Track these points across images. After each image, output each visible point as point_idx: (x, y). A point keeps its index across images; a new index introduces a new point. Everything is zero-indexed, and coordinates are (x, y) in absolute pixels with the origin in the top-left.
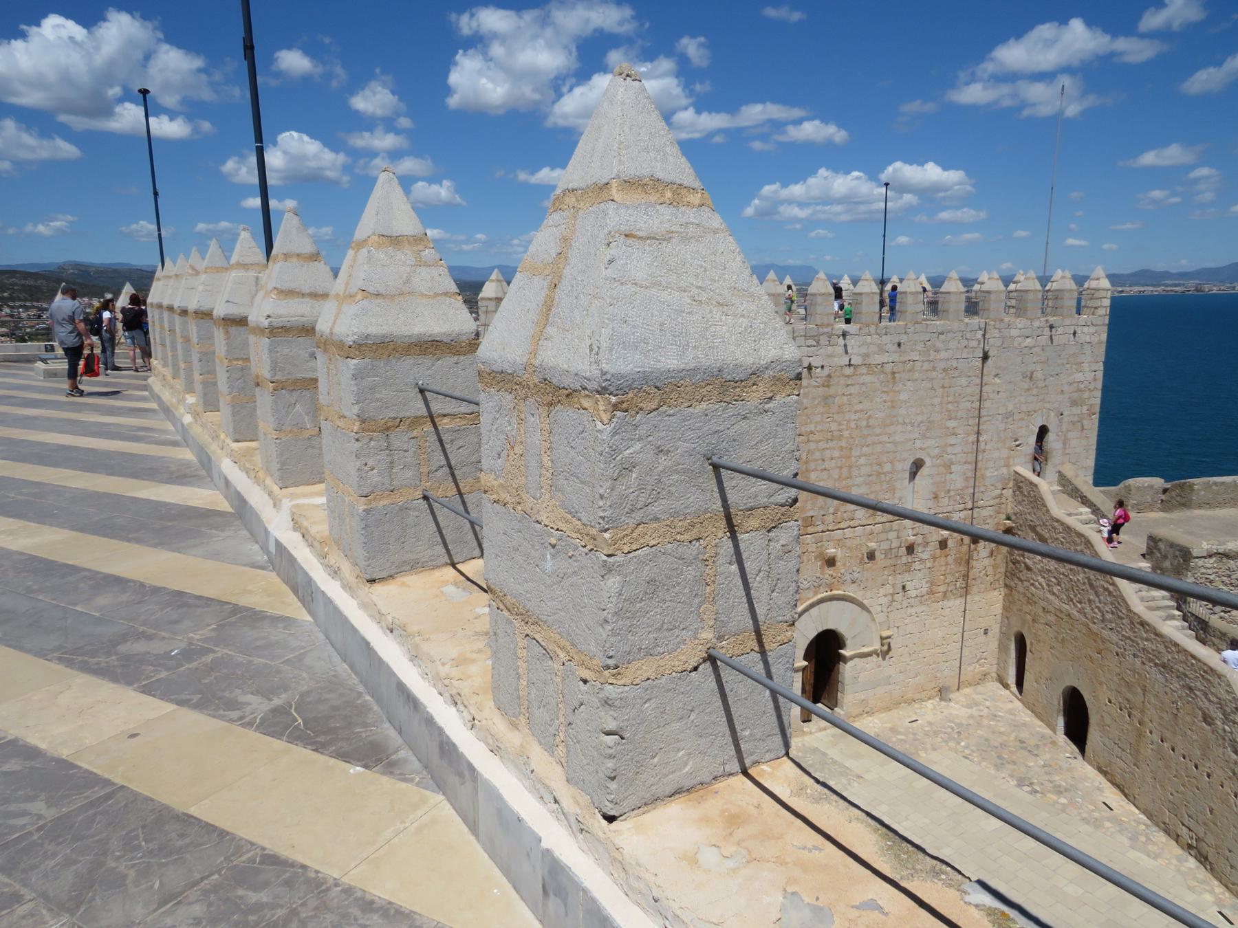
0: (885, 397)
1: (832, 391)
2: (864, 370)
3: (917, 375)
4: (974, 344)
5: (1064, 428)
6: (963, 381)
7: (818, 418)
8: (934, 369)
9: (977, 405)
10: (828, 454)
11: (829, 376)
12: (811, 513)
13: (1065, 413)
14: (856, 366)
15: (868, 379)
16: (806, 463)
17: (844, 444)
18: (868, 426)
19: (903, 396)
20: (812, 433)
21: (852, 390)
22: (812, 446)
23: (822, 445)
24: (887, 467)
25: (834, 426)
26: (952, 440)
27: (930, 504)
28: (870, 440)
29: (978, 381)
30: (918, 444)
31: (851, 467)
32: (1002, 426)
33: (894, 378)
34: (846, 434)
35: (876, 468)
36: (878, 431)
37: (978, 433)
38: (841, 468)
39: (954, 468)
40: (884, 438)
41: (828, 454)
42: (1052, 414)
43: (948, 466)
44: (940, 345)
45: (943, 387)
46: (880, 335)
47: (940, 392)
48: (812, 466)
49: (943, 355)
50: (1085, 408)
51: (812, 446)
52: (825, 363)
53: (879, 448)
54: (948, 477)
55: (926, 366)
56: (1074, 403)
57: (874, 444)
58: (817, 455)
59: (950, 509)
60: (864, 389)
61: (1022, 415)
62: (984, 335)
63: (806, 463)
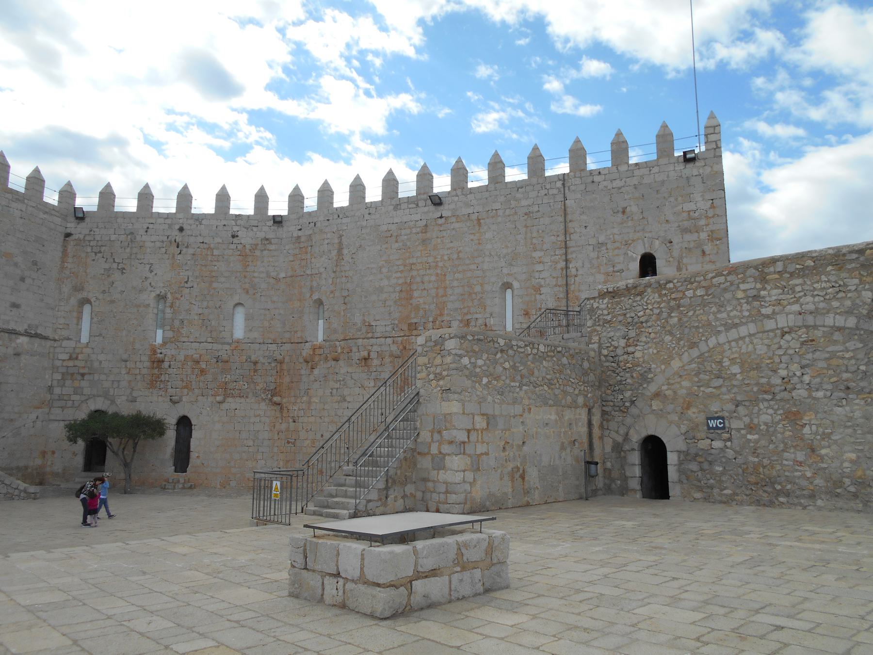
0: (472, 237)
1: (428, 235)
2: (454, 219)
3: (500, 219)
4: (555, 191)
5: (676, 253)
6: (547, 220)
7: (419, 254)
8: (516, 213)
9: (562, 238)
10: (426, 278)
11: (426, 226)
12: (415, 321)
13: (675, 241)
14: (447, 218)
15: (457, 225)
16: (411, 284)
17: (439, 271)
18: (459, 258)
19: (489, 235)
20: (414, 264)
21: (444, 234)
22: (414, 273)
23: (422, 272)
24: (478, 289)
25: (431, 260)
26: (540, 267)
27: (521, 319)
28: (460, 268)
29: (561, 219)
30: (505, 271)
31: (445, 288)
32: (593, 255)
33: (480, 224)
34: (441, 264)
35: (467, 289)
36: (467, 262)
37: (566, 260)
38: (437, 288)
39: (543, 290)
40: (473, 267)
41: (426, 278)
42: (657, 242)
43: (537, 289)
44: (519, 196)
45: (526, 227)
46: (466, 195)
47: (523, 230)
48: (414, 287)
49: (524, 203)
50: (703, 236)
51: (414, 273)
52: (423, 218)
53: (469, 274)
54: (538, 296)
55: (508, 212)
56: (685, 231)
57: (464, 271)
58: (418, 279)
59: (542, 324)
60: (454, 232)
61: (617, 245)
62: (563, 184)
63: (411, 284)
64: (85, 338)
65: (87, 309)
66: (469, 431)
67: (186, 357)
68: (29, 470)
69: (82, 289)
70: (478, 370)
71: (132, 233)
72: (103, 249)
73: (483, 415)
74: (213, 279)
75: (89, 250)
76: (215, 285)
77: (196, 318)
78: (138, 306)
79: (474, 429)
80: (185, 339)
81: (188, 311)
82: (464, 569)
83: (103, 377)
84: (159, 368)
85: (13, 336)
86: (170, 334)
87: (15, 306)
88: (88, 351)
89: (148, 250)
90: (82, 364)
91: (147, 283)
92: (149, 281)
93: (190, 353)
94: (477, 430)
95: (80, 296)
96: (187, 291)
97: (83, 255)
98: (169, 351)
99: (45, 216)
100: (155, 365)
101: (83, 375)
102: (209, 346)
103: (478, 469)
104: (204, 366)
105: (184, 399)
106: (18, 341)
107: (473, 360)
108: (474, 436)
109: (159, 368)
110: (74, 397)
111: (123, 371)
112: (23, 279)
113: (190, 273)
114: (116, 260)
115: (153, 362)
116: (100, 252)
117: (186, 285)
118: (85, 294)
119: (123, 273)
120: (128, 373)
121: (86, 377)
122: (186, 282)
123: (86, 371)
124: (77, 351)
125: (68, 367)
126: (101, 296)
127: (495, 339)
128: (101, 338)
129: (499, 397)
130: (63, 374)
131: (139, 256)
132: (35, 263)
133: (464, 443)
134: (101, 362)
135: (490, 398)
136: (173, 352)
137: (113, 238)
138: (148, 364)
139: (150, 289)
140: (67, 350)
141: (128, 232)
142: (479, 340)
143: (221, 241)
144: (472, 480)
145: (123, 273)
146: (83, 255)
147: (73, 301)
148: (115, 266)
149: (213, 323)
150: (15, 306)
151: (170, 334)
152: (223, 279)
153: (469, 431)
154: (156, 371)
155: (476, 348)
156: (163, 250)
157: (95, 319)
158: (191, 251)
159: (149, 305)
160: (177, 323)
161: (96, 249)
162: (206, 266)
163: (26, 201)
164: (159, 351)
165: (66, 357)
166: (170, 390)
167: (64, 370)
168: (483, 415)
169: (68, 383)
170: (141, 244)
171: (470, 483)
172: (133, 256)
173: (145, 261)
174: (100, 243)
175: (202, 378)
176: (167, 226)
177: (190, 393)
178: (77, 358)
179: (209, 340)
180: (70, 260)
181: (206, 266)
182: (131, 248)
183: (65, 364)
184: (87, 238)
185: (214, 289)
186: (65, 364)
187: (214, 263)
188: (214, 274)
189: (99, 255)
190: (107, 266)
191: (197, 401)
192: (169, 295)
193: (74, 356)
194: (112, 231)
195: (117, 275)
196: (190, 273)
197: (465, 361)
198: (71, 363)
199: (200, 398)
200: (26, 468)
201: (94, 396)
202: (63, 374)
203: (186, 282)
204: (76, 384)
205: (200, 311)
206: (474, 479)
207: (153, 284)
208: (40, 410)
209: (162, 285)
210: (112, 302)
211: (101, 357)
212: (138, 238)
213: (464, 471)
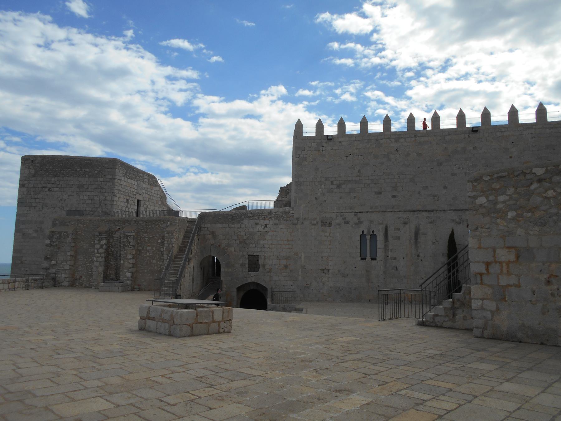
66: (488, 264)
70: (500, 206)
73: (509, 248)
79: (496, 262)
82: (162, 322)
94: (500, 263)
103: (503, 299)
107: (491, 198)
108: (494, 269)
127: (528, 171)
129: (537, 229)
133: (481, 274)
135: (520, 231)
142: (501, 177)
144: (494, 308)
153: (488, 264)
155: (496, 186)
168: (509, 248)
171: (492, 312)
197: (482, 200)
206: (498, 309)
213: (483, 299)
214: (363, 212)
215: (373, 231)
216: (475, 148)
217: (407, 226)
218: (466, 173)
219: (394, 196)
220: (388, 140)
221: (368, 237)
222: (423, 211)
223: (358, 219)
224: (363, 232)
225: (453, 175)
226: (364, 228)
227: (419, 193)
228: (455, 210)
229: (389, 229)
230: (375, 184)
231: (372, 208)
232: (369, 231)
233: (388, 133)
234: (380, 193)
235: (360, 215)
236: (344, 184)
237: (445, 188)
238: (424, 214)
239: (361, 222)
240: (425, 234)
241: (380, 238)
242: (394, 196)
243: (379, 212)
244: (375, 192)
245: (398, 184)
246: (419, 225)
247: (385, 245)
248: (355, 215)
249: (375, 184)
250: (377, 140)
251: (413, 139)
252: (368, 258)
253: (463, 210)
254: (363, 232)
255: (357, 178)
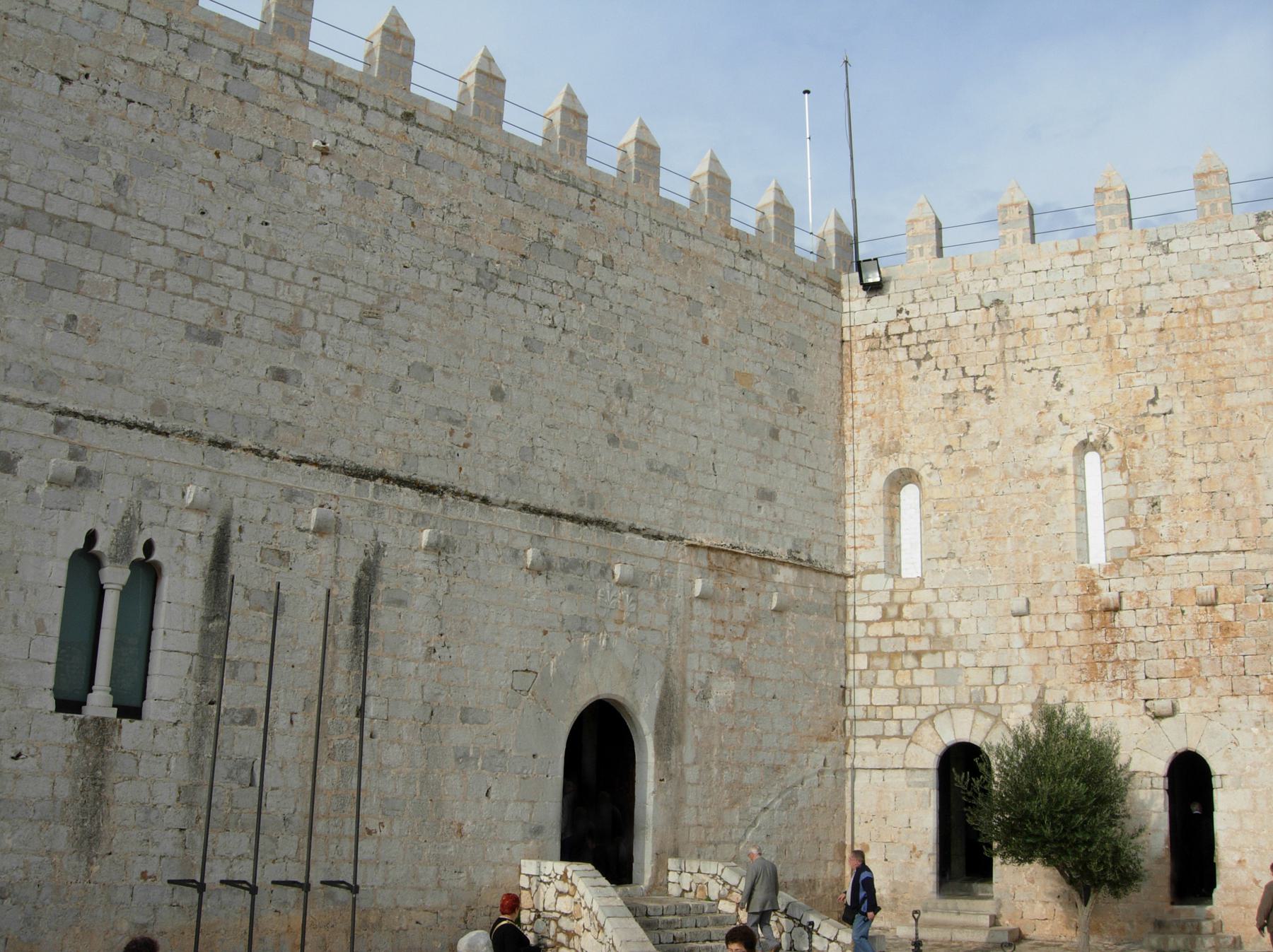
64: (911, 566)
65: (909, 495)
67: (1177, 593)
68: (819, 891)
69: (896, 449)
71: (998, 302)
72: (933, 349)
74: (1224, 385)
75: (901, 354)
76: (1230, 400)
77: (1192, 489)
78: (1034, 475)
80: (1170, 549)
81: (1168, 475)
83: (966, 659)
84: (1108, 627)
85: (768, 567)
86: (1128, 538)
87: (766, 496)
88: (924, 596)
89: (1044, 337)
90: (915, 628)
91: (1051, 417)
92: (1056, 411)
93: (1187, 582)
95: (892, 466)
96: (1158, 424)
97: (889, 370)
98: (1131, 584)
99: (802, 288)
100: (1097, 621)
101: (918, 655)
102: (1238, 562)
104: (1228, 615)
105: (1183, 706)
106: (779, 578)
109: (1108, 627)
110: (899, 712)
111: (1017, 642)
112: (774, 434)
113: (1159, 378)
114: (971, 371)
115: (1091, 613)
116: (928, 357)
117: (1153, 410)
118: (903, 461)
119: (989, 399)
120: (1028, 645)
121: (926, 660)
122: (1153, 402)
123: (924, 645)
124: (899, 598)
125: (879, 638)
126: (942, 462)
128: (954, 563)
130: (870, 655)
131: (1023, 354)
132: (793, 396)
134: (958, 622)
136: (1141, 584)
137: (954, 319)
138: (1078, 620)
139: (1062, 430)
140: (874, 599)
141: (987, 302)
143: (1227, 286)
145: (989, 399)
146: (889, 370)
147: (878, 480)
148: (968, 384)
149: (1240, 499)
150: (766, 496)
151: (1128, 538)
152: (1250, 383)
154: (1100, 637)
156: (1082, 330)
157: (935, 519)
158: (1152, 322)
159: (1062, 471)
160: (1141, 508)
161: (917, 353)
162: (1197, 354)
163: (765, 257)
164: (1102, 585)
165: (875, 614)
166: (1142, 684)
167: (872, 646)
169: (885, 677)
170: (1024, 323)
172: (1009, 356)
173: (1042, 364)
174: (924, 338)
175: (1228, 648)
176: (1080, 272)
177: (1199, 690)
178: (899, 617)
179: (1236, 544)
180: (860, 385)
181: (1197, 354)
182: (1003, 336)
183: (873, 631)
184: (894, 330)
185: (1231, 410)
186: (873, 631)
187: (1218, 344)
188: (1222, 372)
189: (927, 365)
190: (949, 387)
191: (1219, 710)
192: (1112, 440)
193: (893, 612)
194: (948, 305)
195: (976, 405)
196: (1159, 378)
198: (886, 629)
199: (1227, 701)
200: (812, 883)
201: (949, 707)
202: (870, 655)
203: (1153, 402)
204: (903, 679)
205: (1200, 471)
207: (1066, 417)
208: (830, 744)
209: (1091, 416)
210: (972, 471)
211: (958, 609)
212: (1015, 311)
214: (104, 421)
215: (149, 547)
216: (608, 262)
217: (325, 546)
218: (572, 353)
219: (280, 375)
220: (287, 81)
221: (114, 577)
222: (402, 482)
223: (74, 455)
224: (91, 537)
225: (530, 344)
226: (98, 514)
227: (396, 388)
228: (525, 508)
229: (235, 548)
230: (196, 280)
231: (158, 407)
232: (124, 543)
233: (291, 50)
234: (214, 338)
235: (88, 433)
236: (21, 225)
237: (498, 394)
238: (408, 498)
239: (84, 478)
240: (401, 603)
241: (180, 593)
242: (280, 375)
243: (193, 436)
244: (189, 326)
245: (308, 320)
246: (379, 550)
247: (206, 634)
248: (59, 428)
249: (196, 280)
250: (234, 57)
251: (397, 126)
252: (99, 702)
253: (549, 514)
254: (91, 537)
255: (104, 220)
